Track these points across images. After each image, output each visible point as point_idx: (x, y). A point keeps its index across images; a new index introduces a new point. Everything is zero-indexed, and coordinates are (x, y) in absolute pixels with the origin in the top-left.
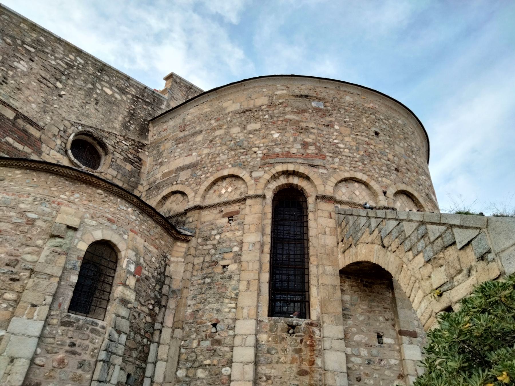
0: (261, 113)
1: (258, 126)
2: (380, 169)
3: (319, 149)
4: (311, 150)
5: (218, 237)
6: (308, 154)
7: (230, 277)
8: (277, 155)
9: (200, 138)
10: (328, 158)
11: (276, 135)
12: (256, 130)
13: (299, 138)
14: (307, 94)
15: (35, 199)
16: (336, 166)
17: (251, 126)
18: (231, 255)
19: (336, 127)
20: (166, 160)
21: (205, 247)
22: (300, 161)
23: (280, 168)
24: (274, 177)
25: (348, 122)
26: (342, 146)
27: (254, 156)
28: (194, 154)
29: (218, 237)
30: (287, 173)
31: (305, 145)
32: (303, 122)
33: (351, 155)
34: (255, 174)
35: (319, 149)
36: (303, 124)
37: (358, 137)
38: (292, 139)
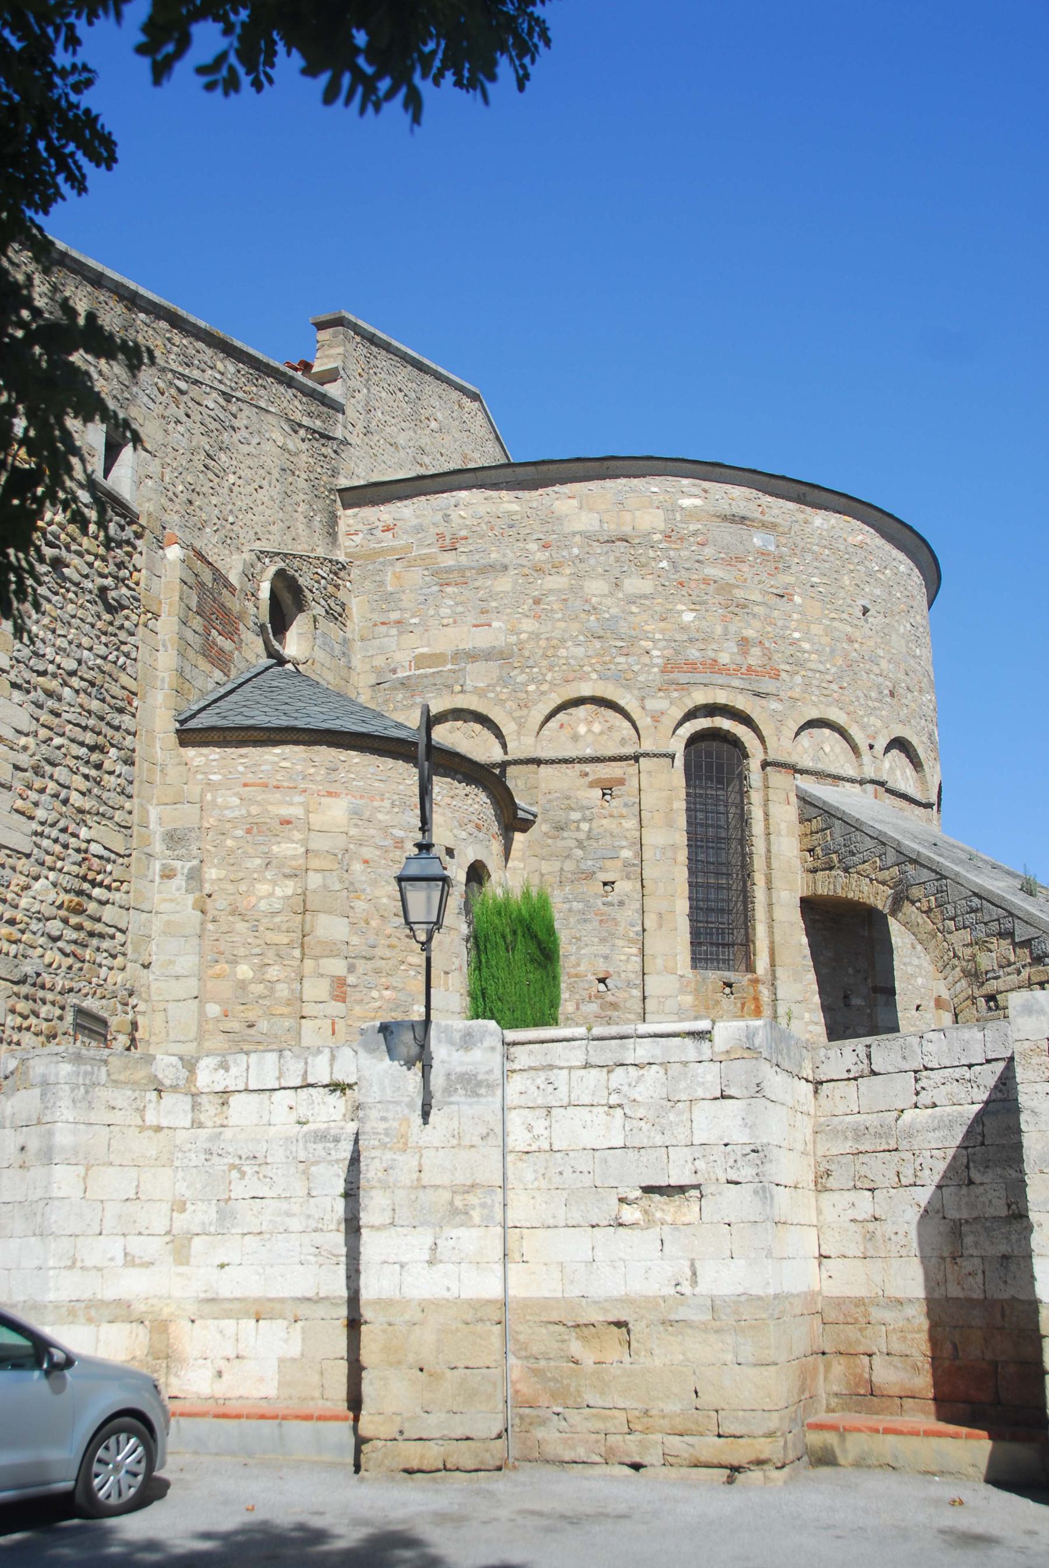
0: (651, 553)
1: (646, 586)
3: (768, 654)
4: (755, 656)
5: (585, 826)
6: (749, 667)
7: (621, 903)
8: (692, 667)
9: (504, 584)
10: (783, 675)
11: (688, 617)
12: (645, 597)
13: (732, 628)
14: (742, 513)
16: (797, 693)
17: (634, 584)
18: (619, 864)
19: (797, 599)
20: (415, 620)
21: (560, 843)
22: (736, 683)
23: (701, 697)
24: (691, 715)
26: (806, 646)
27: (646, 659)
28: (495, 624)
29: (585, 826)
30: (712, 710)
31: (744, 643)
32: (738, 587)
33: (821, 667)
34: (652, 704)
35: (768, 654)
36: (739, 593)
37: (836, 624)
38: (719, 630)
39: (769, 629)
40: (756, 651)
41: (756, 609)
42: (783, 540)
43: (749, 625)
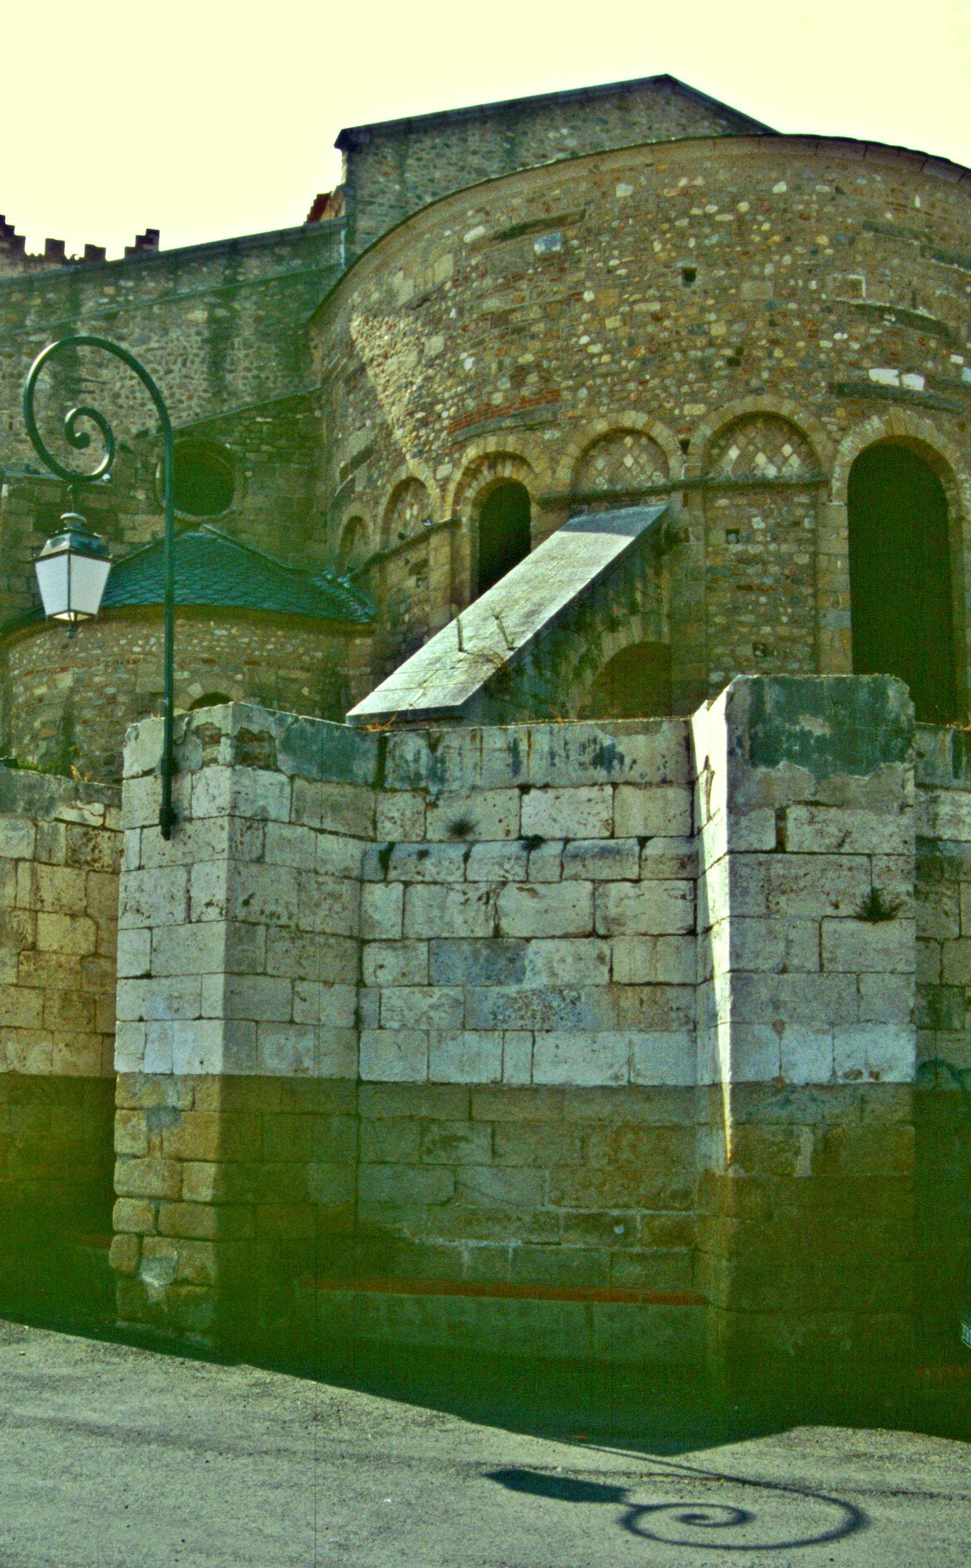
2: (680, 383)
6: (523, 398)
10: (566, 395)
13: (507, 361)
15: (107, 666)
23: (472, 452)
24: (472, 472)
25: (617, 268)
26: (595, 349)
31: (519, 374)
32: (514, 310)
33: (615, 368)
36: (516, 317)
39: (550, 345)
40: (533, 378)
41: (535, 329)
42: (570, 233)
43: (525, 350)
